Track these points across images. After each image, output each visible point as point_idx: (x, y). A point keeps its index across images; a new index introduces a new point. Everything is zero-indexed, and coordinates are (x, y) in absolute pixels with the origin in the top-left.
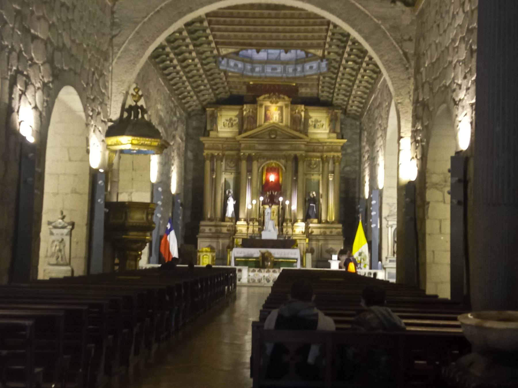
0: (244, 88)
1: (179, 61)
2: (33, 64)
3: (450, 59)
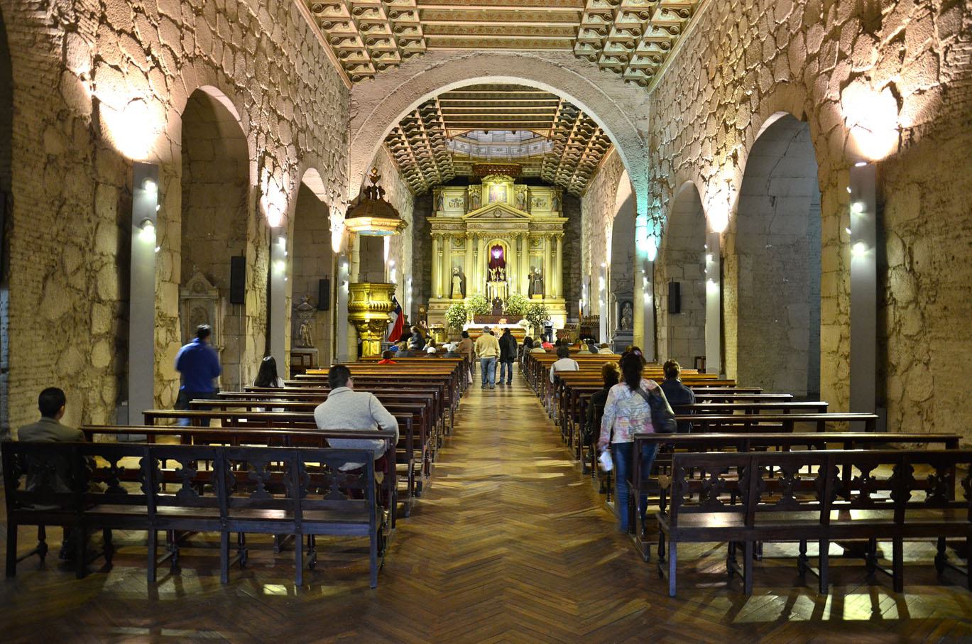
0: (469, 168)
1: (409, 142)
2: (279, 144)
3: (696, 136)
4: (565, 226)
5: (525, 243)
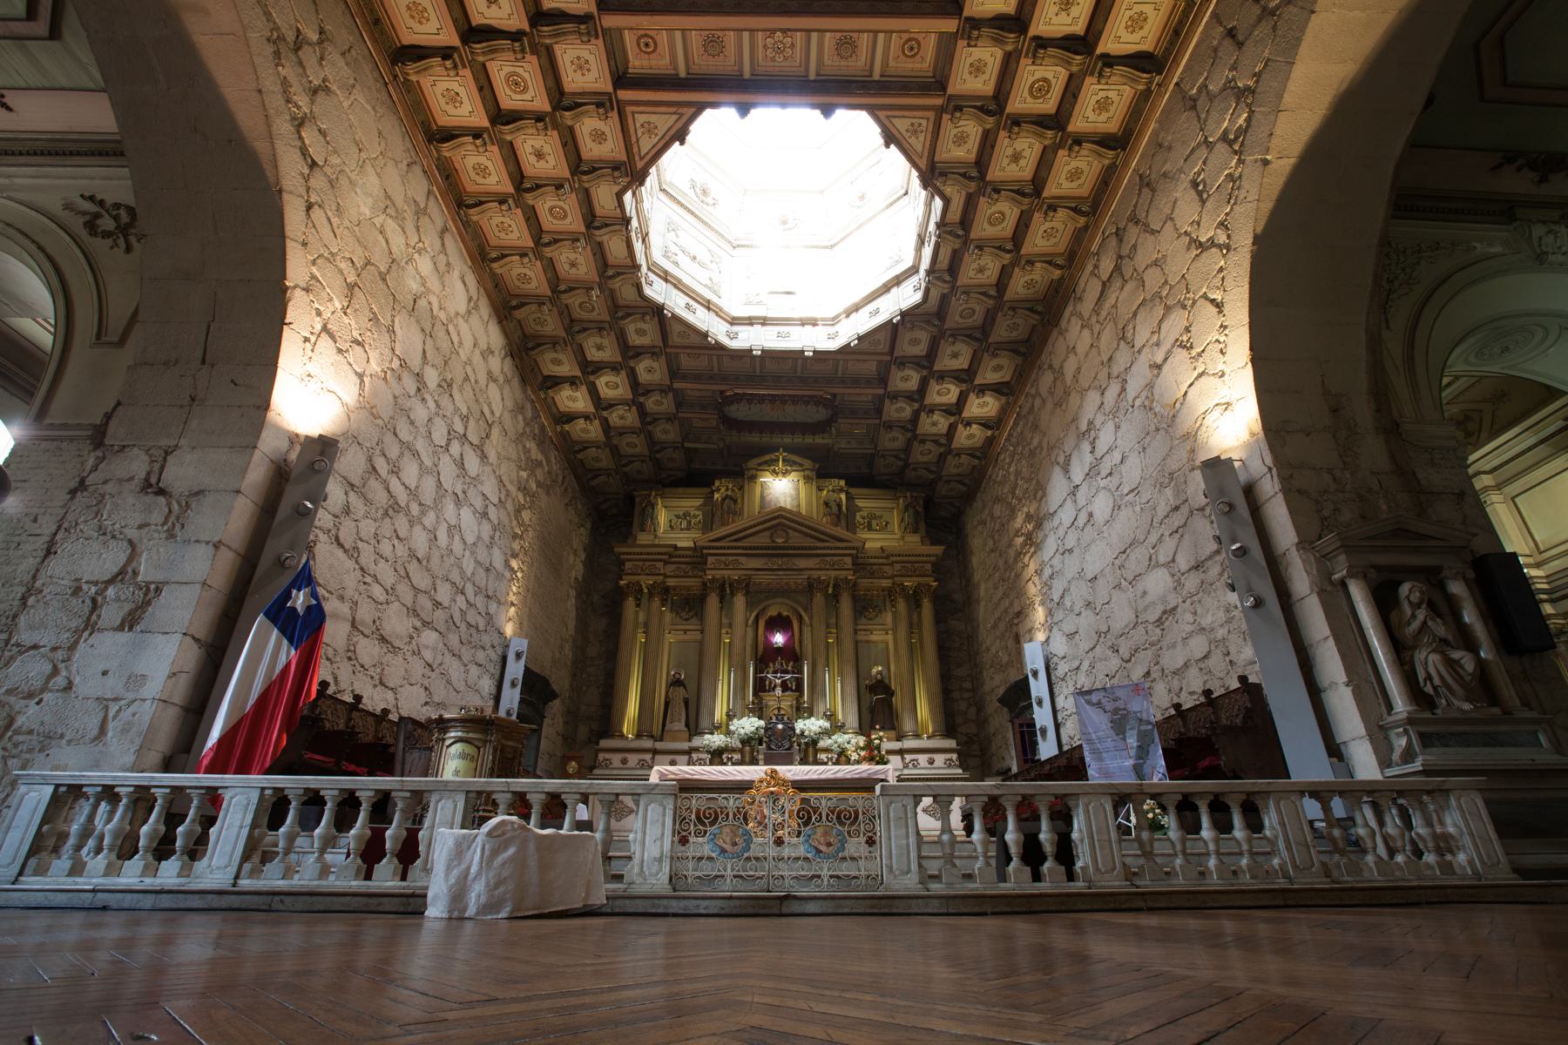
4: (938, 569)
5: (846, 605)
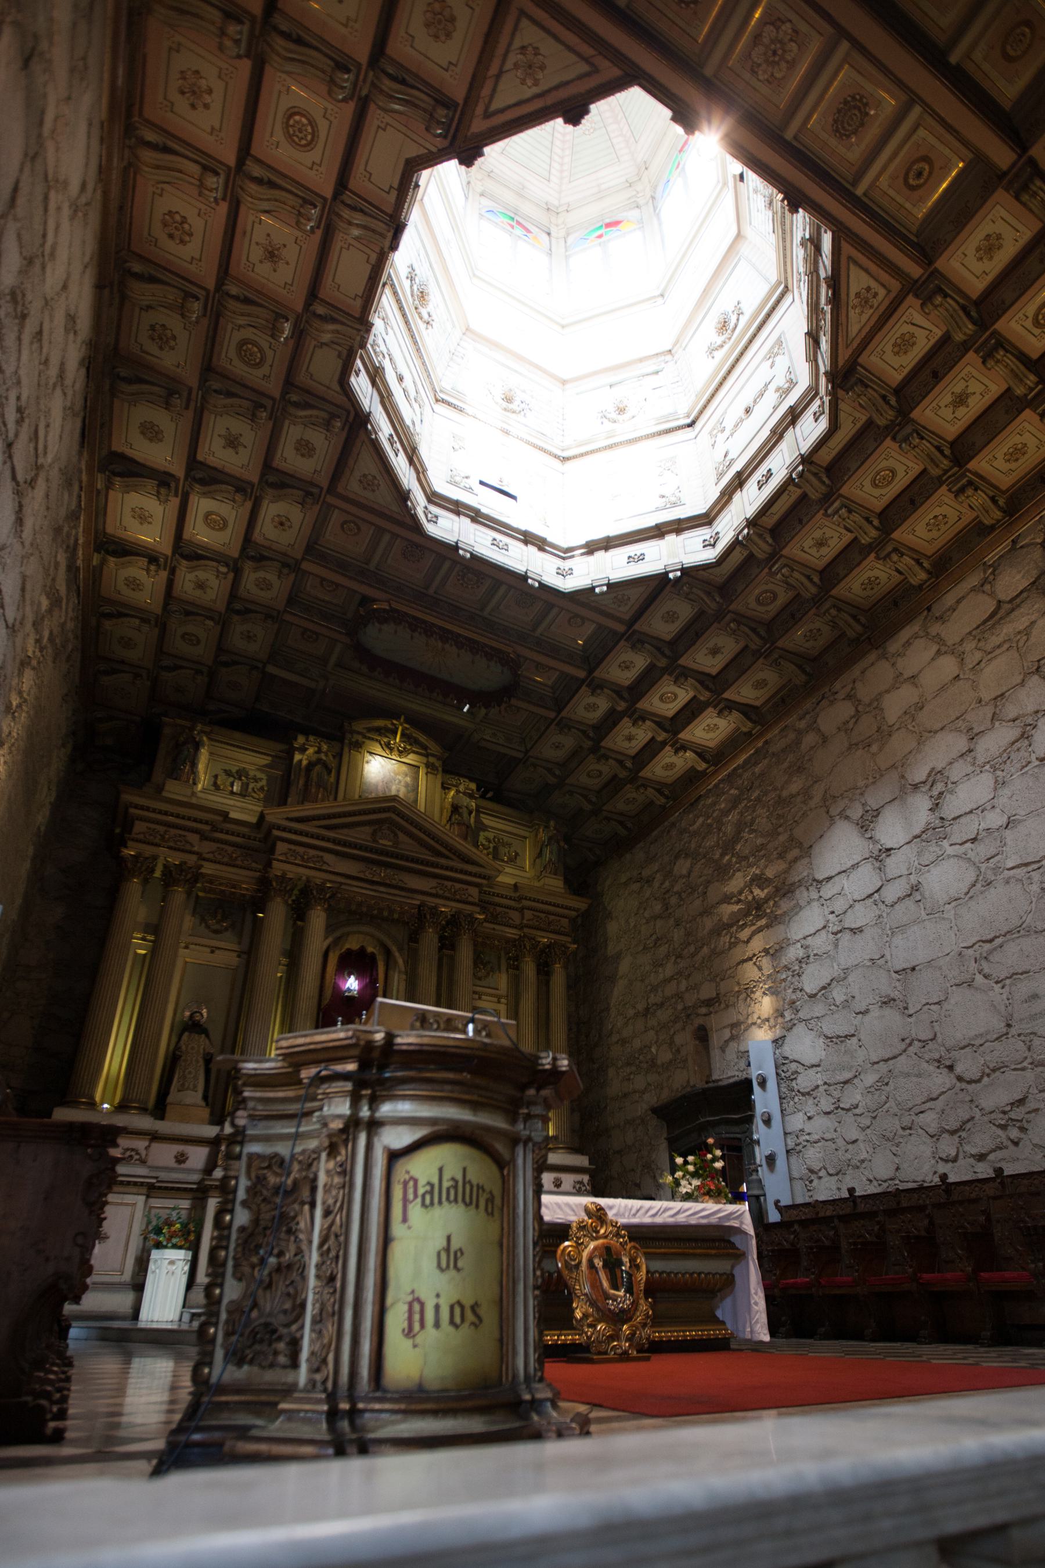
5: (465, 954)
